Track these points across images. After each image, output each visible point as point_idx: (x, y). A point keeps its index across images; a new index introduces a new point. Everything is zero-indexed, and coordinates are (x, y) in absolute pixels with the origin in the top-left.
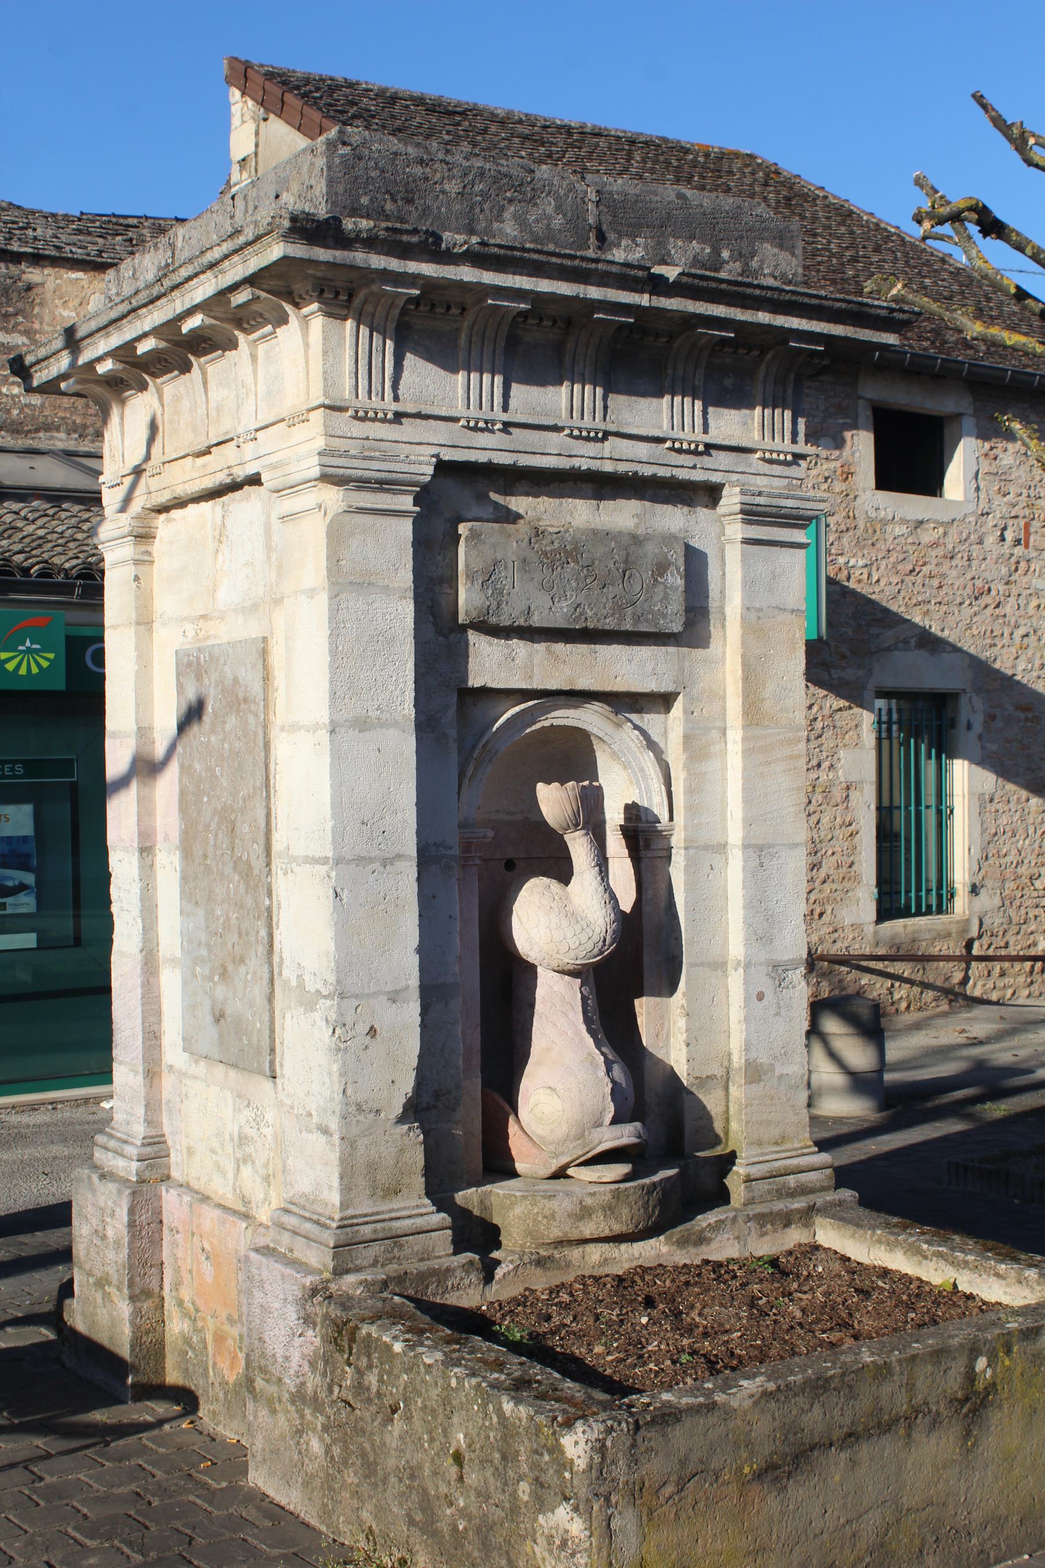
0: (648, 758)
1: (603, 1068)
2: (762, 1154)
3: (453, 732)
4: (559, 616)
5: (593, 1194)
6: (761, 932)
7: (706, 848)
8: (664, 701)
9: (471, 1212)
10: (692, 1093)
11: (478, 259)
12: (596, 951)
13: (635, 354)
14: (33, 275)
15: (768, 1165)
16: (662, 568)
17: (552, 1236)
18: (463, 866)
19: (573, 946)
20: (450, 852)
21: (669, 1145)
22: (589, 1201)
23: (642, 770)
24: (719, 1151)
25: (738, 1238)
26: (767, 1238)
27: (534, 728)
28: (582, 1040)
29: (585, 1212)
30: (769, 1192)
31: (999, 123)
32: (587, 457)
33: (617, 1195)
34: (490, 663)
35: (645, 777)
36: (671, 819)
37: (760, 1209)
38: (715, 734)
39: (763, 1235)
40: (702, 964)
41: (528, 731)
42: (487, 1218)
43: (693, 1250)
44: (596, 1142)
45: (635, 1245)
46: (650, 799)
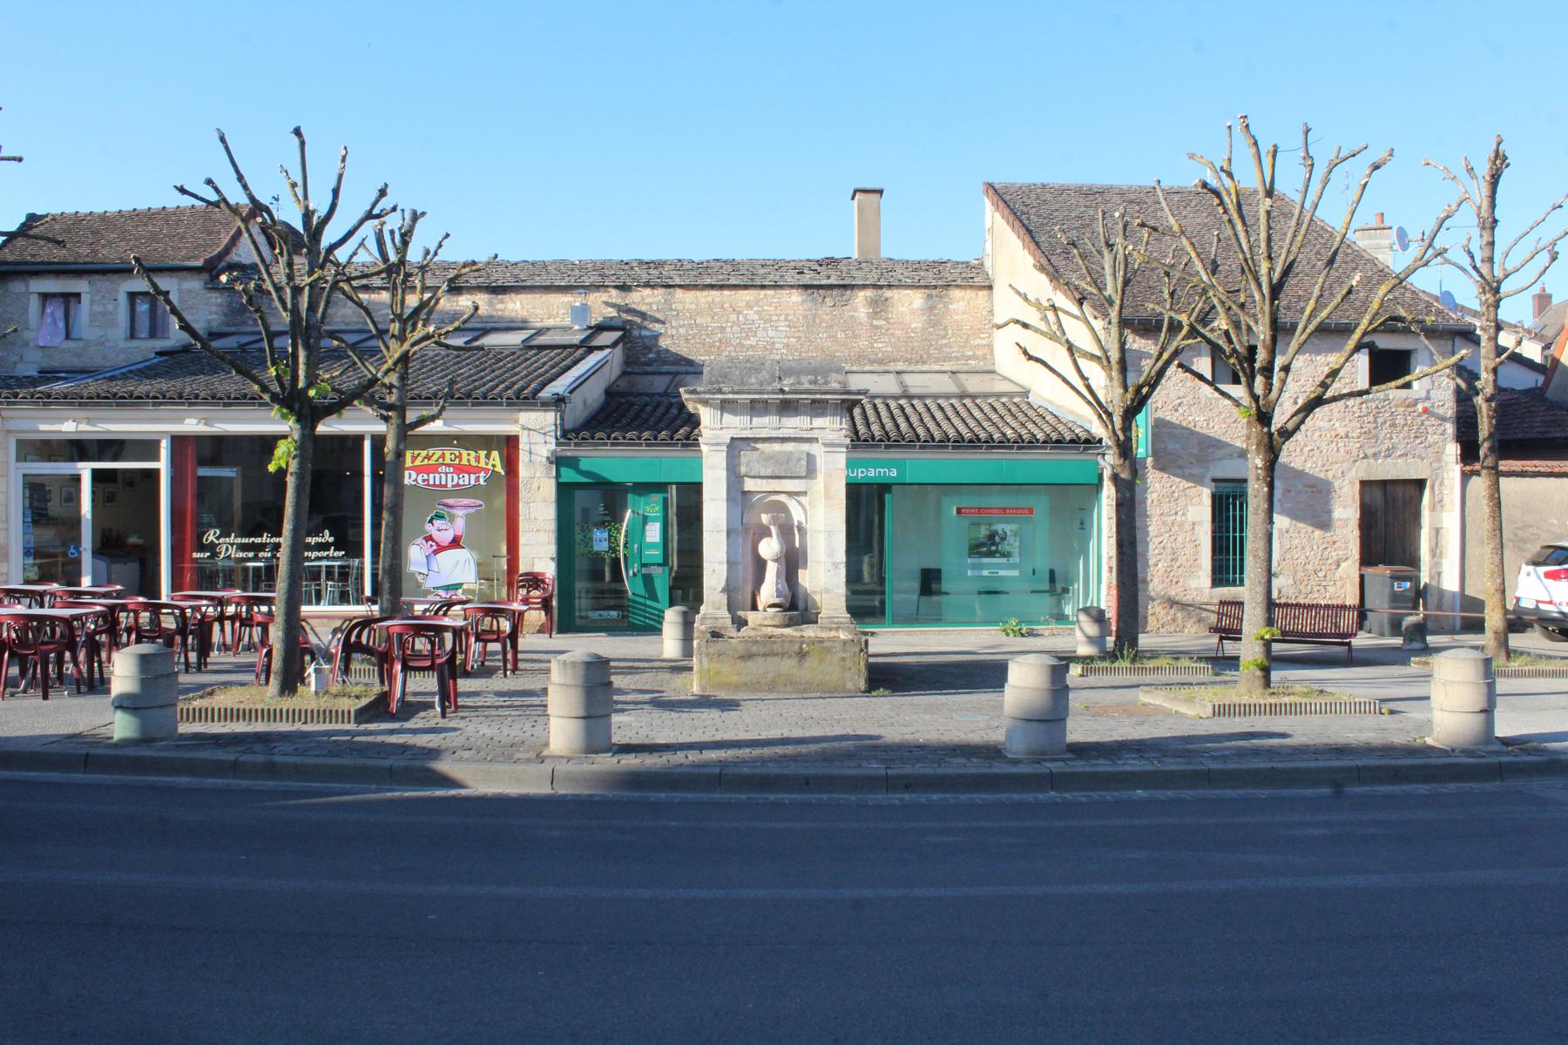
4: (769, 472)
6: (831, 554)
8: (805, 493)
11: (733, 392)
13: (787, 407)
14: (888, 293)
16: (799, 460)
21: (796, 608)
31: (1019, 293)
32: (774, 434)
34: (750, 485)
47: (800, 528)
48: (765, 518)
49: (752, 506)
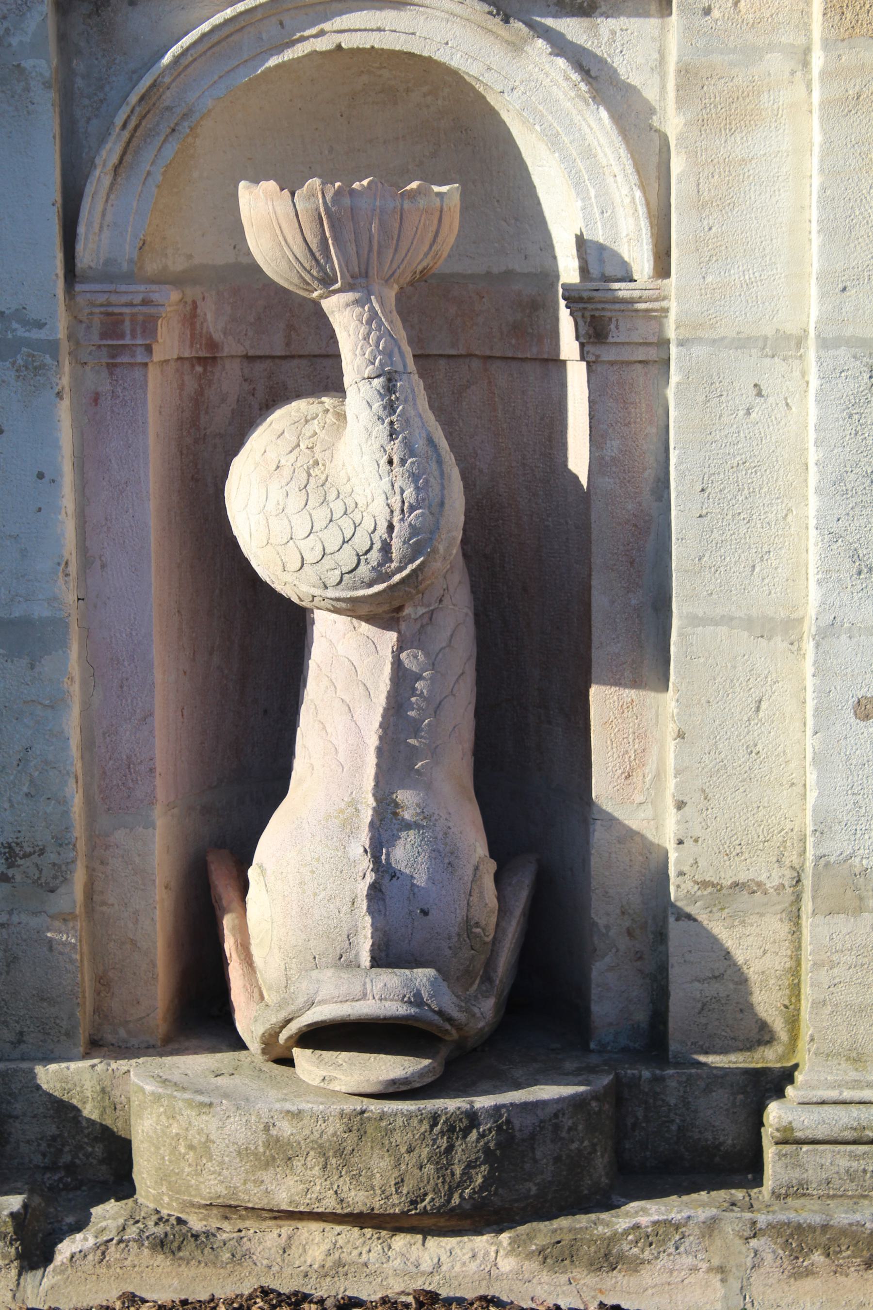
0: (597, 125)
2: (856, 1084)
3: (43, 65)
5: (297, 1115)
7: (743, 343)
9: (78, 1111)
10: (689, 917)
15: (854, 1111)
17: (205, 1192)
18: (111, 367)
19: (310, 558)
20: (36, 335)
22: (285, 1129)
23: (588, 153)
24: (768, 1058)
25: (721, 1270)
26: (808, 1283)
27: (289, 55)
29: (277, 1153)
30: (851, 1175)
33: (357, 1123)
36: (662, 268)
37: (807, 1213)
38: (776, 64)
39: (799, 1274)
40: (728, 620)
41: (273, 62)
42: (118, 1127)
43: (587, 1280)
44: (301, 1001)
45: (432, 1242)
48: (270, 222)
49: (160, 116)
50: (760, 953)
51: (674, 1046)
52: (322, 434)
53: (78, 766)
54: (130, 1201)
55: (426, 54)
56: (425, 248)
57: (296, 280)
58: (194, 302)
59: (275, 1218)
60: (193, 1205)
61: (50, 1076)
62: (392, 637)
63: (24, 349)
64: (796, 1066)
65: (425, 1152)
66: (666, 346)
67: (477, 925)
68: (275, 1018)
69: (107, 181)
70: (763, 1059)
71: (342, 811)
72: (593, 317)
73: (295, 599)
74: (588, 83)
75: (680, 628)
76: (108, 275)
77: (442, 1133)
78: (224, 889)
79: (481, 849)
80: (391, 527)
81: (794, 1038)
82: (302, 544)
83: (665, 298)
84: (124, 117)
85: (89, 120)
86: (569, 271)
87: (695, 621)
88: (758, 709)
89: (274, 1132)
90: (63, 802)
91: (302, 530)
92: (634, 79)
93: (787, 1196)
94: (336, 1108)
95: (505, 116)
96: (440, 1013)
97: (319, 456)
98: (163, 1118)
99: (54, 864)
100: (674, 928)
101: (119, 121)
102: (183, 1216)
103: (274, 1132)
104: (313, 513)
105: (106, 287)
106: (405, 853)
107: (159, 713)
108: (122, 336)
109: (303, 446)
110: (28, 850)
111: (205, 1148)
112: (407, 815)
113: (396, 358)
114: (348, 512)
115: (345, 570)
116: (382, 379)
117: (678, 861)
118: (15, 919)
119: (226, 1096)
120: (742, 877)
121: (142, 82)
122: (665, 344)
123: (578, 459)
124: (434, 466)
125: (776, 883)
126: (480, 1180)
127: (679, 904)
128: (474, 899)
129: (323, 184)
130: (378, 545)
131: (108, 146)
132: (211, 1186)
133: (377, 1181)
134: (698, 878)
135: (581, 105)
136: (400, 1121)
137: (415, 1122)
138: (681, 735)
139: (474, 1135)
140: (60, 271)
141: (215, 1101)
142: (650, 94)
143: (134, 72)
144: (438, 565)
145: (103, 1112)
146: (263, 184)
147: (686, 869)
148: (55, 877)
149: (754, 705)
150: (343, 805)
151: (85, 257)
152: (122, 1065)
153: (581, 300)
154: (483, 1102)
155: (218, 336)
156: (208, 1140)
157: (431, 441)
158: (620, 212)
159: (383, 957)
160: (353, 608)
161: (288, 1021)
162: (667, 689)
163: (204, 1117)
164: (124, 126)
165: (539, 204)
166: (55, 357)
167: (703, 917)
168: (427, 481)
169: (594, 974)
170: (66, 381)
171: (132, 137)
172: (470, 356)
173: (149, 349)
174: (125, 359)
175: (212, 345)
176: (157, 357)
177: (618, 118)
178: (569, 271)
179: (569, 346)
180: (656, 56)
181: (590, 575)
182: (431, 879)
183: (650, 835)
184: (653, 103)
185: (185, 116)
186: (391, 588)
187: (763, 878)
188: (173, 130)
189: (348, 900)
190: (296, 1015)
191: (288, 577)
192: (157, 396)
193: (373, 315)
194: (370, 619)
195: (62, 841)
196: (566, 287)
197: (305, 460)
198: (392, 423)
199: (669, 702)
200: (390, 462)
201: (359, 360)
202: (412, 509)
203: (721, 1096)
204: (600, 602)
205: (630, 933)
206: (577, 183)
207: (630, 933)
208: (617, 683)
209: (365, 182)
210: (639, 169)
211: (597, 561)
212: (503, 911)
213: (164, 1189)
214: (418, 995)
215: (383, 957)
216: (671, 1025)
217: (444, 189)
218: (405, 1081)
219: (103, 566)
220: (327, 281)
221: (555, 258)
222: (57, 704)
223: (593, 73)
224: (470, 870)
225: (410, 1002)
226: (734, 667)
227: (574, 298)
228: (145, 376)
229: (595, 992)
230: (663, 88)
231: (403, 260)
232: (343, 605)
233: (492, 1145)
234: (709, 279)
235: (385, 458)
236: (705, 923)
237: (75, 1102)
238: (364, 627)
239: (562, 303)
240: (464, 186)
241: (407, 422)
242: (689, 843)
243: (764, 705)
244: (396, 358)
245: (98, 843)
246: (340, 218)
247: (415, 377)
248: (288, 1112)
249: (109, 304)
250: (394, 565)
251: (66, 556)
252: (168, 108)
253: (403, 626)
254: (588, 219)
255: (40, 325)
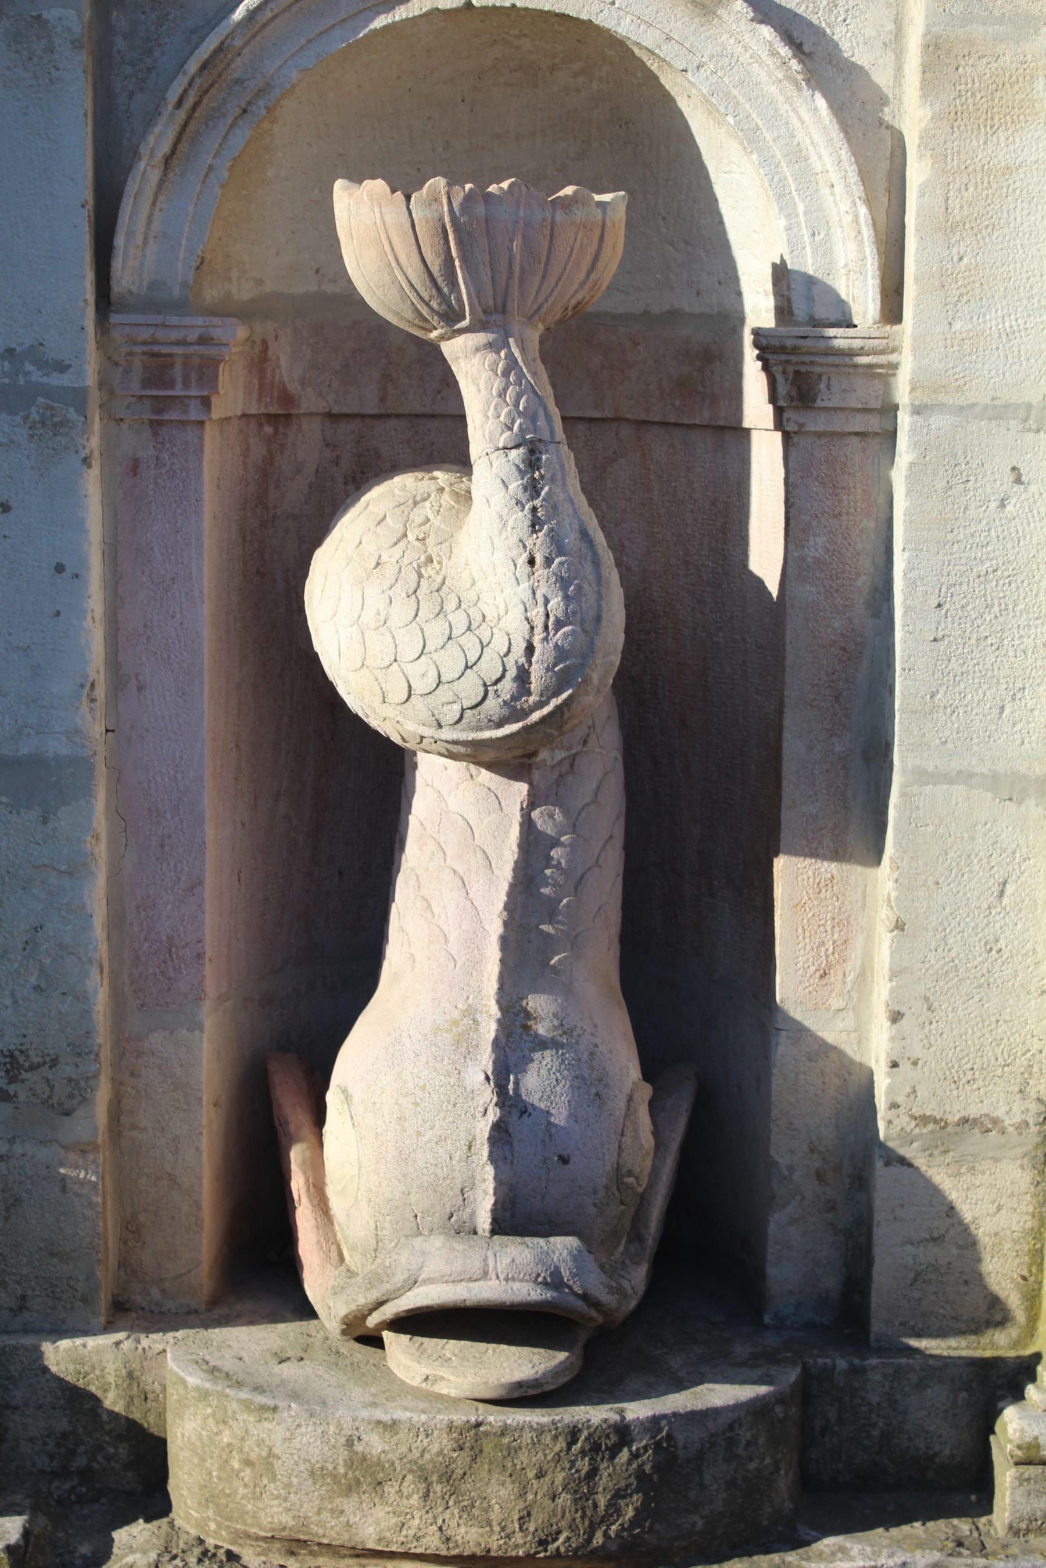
0: (812, 118)
1: (486, 1059)
5: (391, 1427)
7: (997, 412)
10: (903, 1162)
12: (493, 706)
17: (265, 1521)
18: (156, 425)
19: (419, 687)
20: (56, 380)
22: (375, 1444)
23: (797, 155)
24: (999, 1344)
28: (476, 964)
29: (363, 1475)
33: (471, 1439)
35: (807, 178)
40: (965, 777)
41: (380, 22)
42: (150, 1422)
44: (399, 1278)
46: (824, 248)
47: (809, 365)
48: (376, 236)
49: (228, 92)
50: (992, 1209)
51: (877, 1327)
52: (436, 521)
53: (102, 950)
54: (164, 1521)
55: (584, 16)
56: (582, 276)
57: (409, 315)
58: (264, 342)
59: (357, 1556)
60: (248, 1536)
61: (61, 1355)
62: (522, 788)
63: (41, 400)
64: (1037, 1357)
65: (560, 1477)
66: (891, 415)
67: (630, 1173)
68: (363, 1299)
69: (155, 176)
70: (993, 1345)
71: (455, 1023)
72: (797, 373)
73: (396, 739)
74: (800, 61)
75: (903, 786)
76: (155, 303)
77: (583, 1453)
78: (293, 1112)
79: (634, 1072)
80: (530, 649)
81: (1033, 1319)
82: (409, 669)
83: (894, 350)
84: (179, 91)
85: (131, 95)
86: (759, 309)
87: (921, 777)
88: (1002, 894)
89: (359, 1448)
90: (84, 998)
91: (409, 648)
92: (861, 58)
93: (1028, 1531)
94: (443, 1418)
95: (683, 104)
96: (585, 1297)
97: (432, 551)
98: (211, 1422)
99: (70, 1080)
100: (882, 1175)
101: (172, 97)
102: (235, 1549)
103: (359, 1448)
104: (427, 628)
105: (151, 319)
106: (540, 1081)
107: (210, 880)
108: (171, 385)
109: (411, 537)
110: (36, 1060)
111: (267, 1465)
112: (542, 1029)
113: (541, 422)
114: (473, 627)
115: (467, 704)
116: (522, 450)
117: (890, 1090)
118: (18, 1149)
119: (295, 1396)
120: (973, 1112)
121: (205, 44)
122: (892, 410)
123: (766, 557)
124: (589, 568)
125: (1018, 1119)
126: (630, 1513)
127: (891, 1144)
128: (627, 1140)
129: (449, 185)
130: (512, 672)
131: (157, 129)
132: (274, 1514)
133: (496, 1514)
134: (916, 1111)
135: (790, 89)
136: (528, 1437)
137: (547, 1439)
138: (899, 926)
139: (624, 1455)
140: (90, 296)
141: (282, 1404)
142: (882, 78)
143: (193, 32)
144: (589, 699)
145: (130, 1404)
146: (367, 183)
147: (900, 1099)
148: (71, 1096)
149: (996, 889)
150: (456, 1014)
151: (125, 276)
152: (154, 1341)
153: (782, 349)
154: (637, 1410)
155: (293, 387)
156: (271, 1454)
157: (584, 534)
158: (837, 234)
159: (510, 1220)
160: (475, 754)
161: (380, 1304)
162: (879, 862)
163: (267, 1425)
164: (179, 104)
165: (721, 222)
166: (82, 408)
167: (920, 1162)
168: (579, 588)
169: (772, 1228)
170: (94, 442)
171: (189, 117)
172: (618, 419)
173: (206, 403)
174: (173, 415)
175: (287, 399)
176: (217, 413)
177: (838, 109)
178: (759, 309)
179: (756, 406)
180: (891, 27)
181: (780, 713)
182: (573, 1116)
183: (851, 1050)
184: (885, 90)
185: (261, 92)
186: (526, 729)
187: (1000, 1113)
188: (245, 111)
189: (463, 1143)
190: (393, 1296)
191: (389, 711)
192: (215, 464)
193: (512, 364)
194: (491, 767)
195: (81, 1050)
196: (757, 333)
197: (414, 555)
198: (534, 509)
199: (883, 878)
200: (531, 562)
201: (492, 425)
202: (559, 624)
203: (938, 1394)
204: (794, 747)
205: (820, 1176)
206: (781, 196)
207: (820, 1176)
208: (813, 853)
209: (505, 185)
210: (865, 176)
211: (791, 694)
212: (660, 1146)
213: (210, 1513)
214: (556, 1273)
215: (510, 1220)
216: (874, 1299)
217: (607, 197)
218: (535, 1383)
219: (141, 688)
220: (451, 316)
221: (739, 294)
222: (77, 869)
223: (806, 49)
224: (622, 1103)
225: (545, 1283)
226: (972, 839)
227: (768, 348)
228: (201, 438)
229: (772, 1250)
230: (899, 70)
231: (552, 291)
232: (462, 749)
233: (647, 1468)
234: (957, 326)
235: (525, 557)
236: (923, 1169)
237: (93, 1389)
238: (485, 776)
239: (750, 353)
240: (631, 193)
241: (554, 509)
242: (905, 1066)
243: (1009, 889)
244: (541, 422)
245: (127, 1048)
246: (472, 233)
247: (564, 448)
248: (379, 1422)
249: (155, 342)
250: (532, 699)
251: (92, 675)
252: (238, 81)
253: (536, 775)
254: (794, 243)
255: (62, 368)
